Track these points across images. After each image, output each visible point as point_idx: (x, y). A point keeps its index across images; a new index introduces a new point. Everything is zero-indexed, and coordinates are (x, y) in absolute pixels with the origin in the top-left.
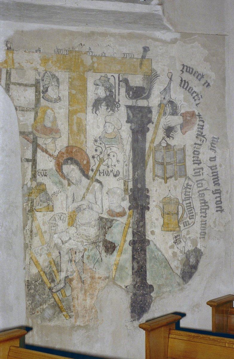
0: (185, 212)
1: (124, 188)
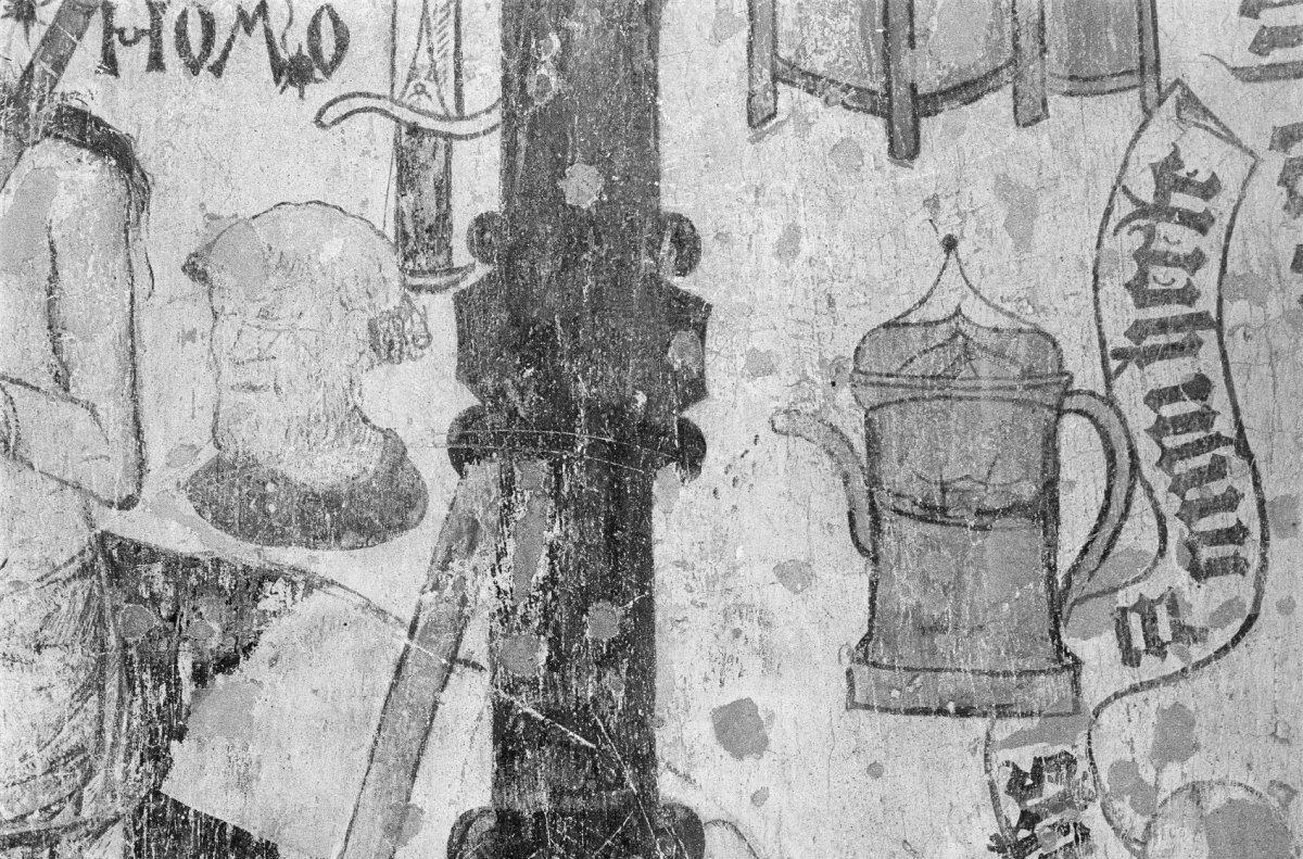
0: (1139, 490)
1: (399, 216)
